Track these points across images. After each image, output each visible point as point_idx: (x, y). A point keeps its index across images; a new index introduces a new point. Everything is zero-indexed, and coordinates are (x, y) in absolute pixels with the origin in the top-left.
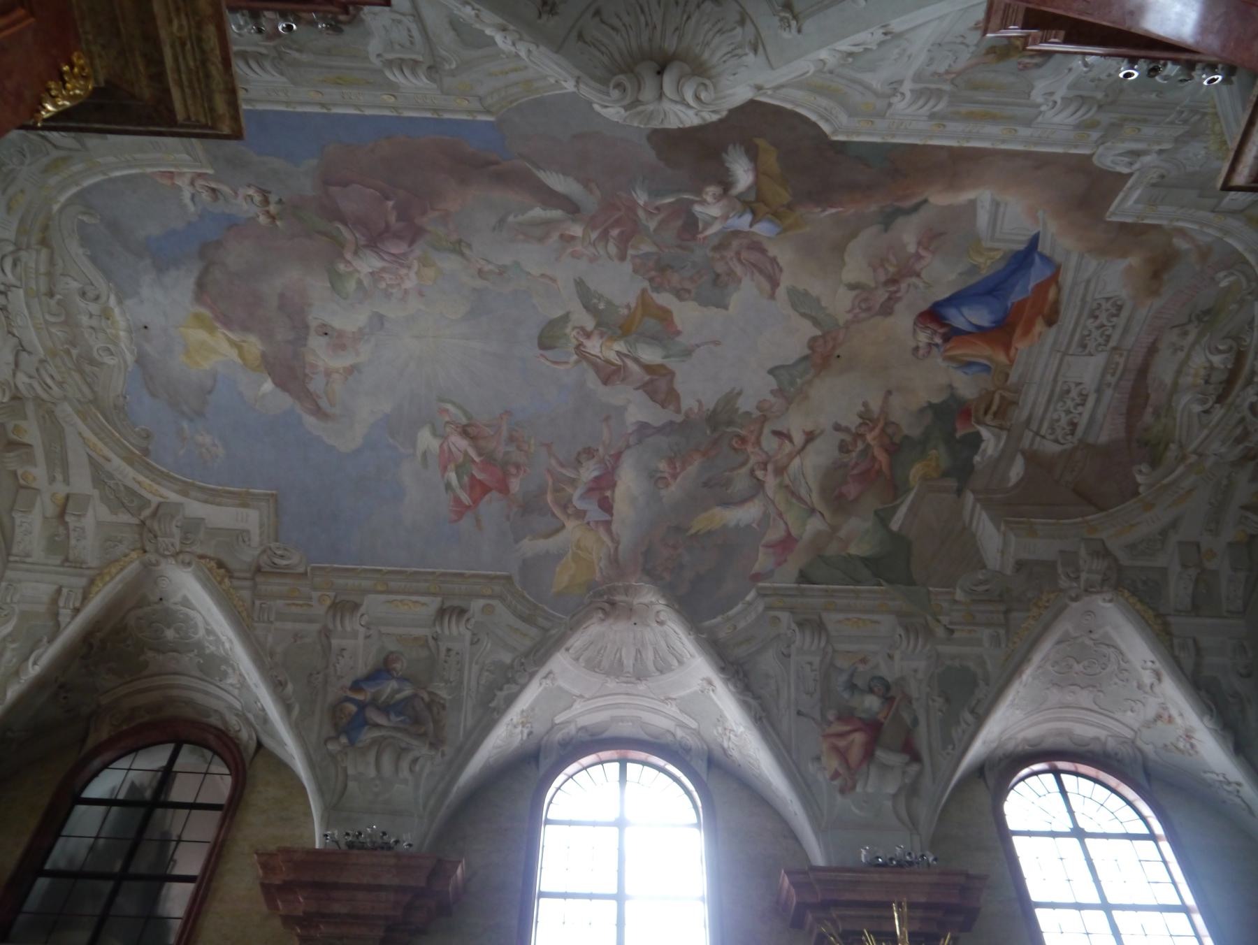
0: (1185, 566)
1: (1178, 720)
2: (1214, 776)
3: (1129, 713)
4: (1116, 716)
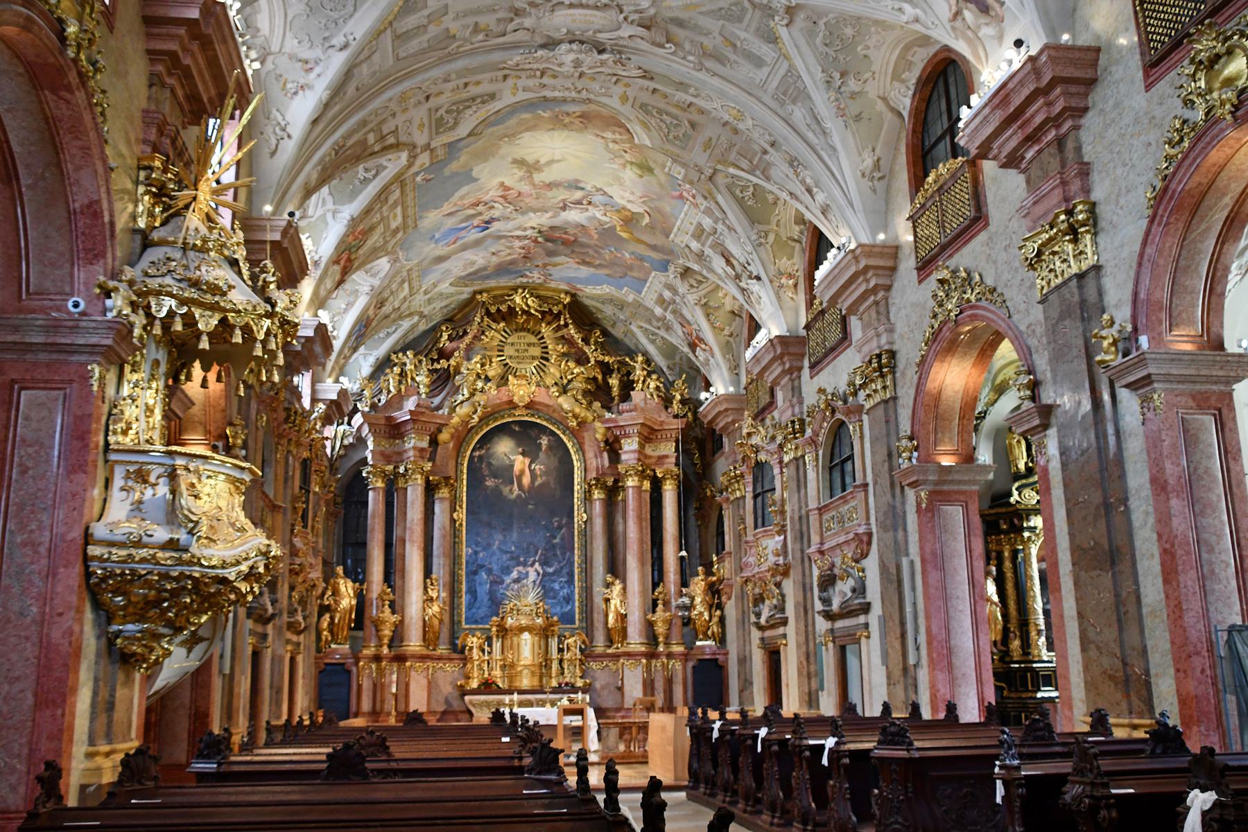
0: (429, 16)
1: (313, 75)
2: (280, 118)
3: (296, 41)
4: (288, 34)
